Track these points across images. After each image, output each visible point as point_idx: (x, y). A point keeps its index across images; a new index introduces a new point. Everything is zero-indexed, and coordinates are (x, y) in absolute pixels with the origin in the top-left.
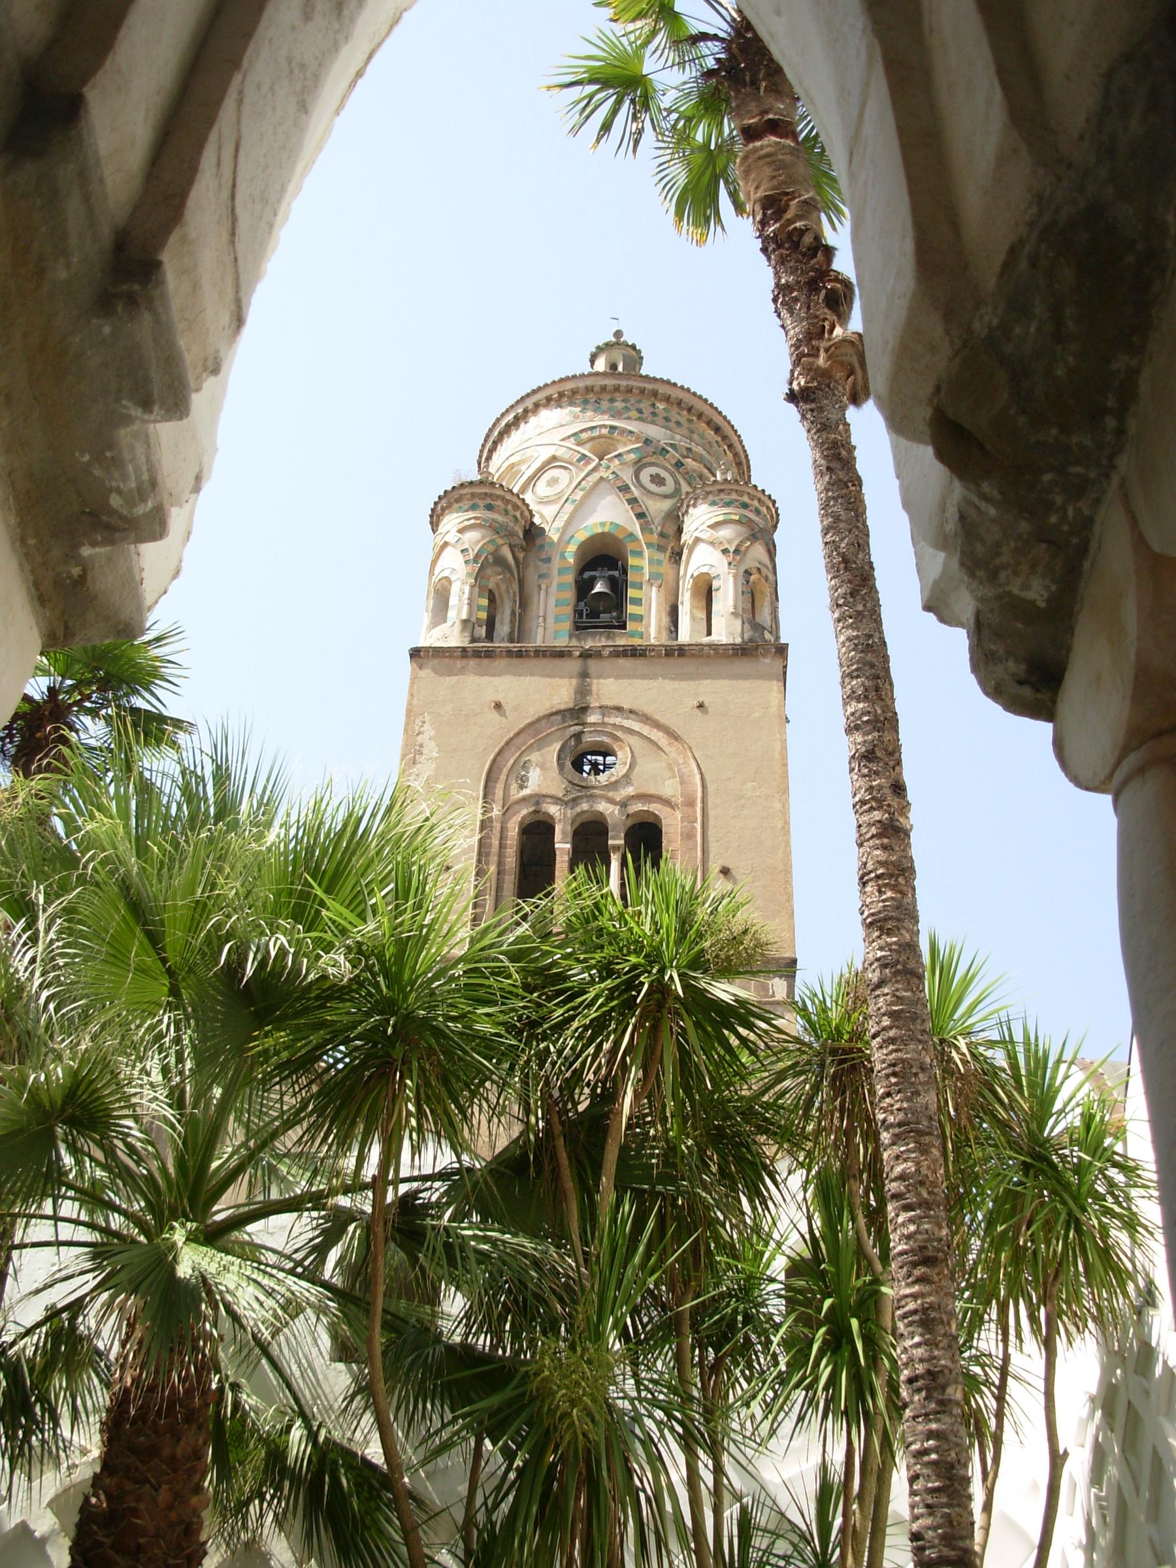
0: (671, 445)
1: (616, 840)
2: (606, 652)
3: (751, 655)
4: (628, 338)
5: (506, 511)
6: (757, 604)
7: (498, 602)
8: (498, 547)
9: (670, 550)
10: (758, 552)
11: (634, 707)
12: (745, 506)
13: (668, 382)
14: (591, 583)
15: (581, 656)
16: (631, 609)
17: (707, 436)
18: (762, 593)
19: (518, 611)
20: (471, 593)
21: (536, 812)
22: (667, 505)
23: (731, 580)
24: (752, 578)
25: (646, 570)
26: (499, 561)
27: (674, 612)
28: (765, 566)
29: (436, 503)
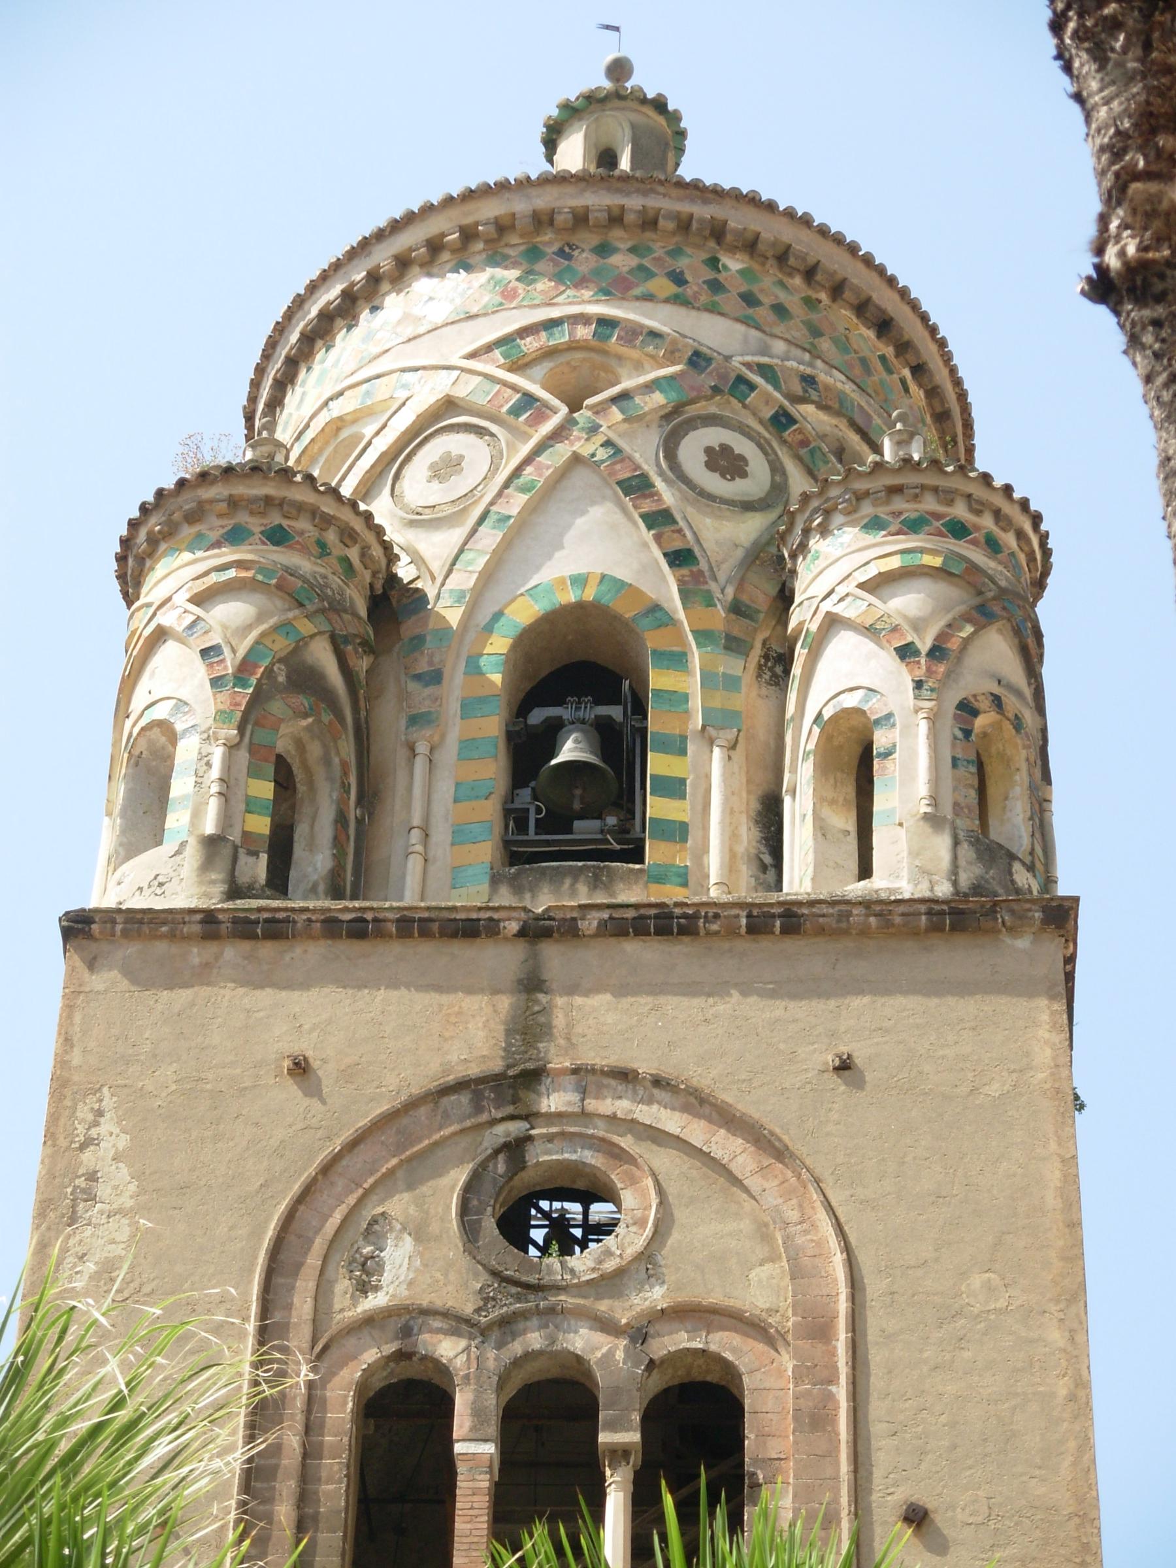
0: (765, 371)
1: (620, 1433)
2: (589, 925)
3: (979, 930)
4: (646, 80)
5: (322, 545)
6: (992, 791)
7: (301, 788)
8: (302, 644)
9: (757, 652)
10: (995, 651)
12: (958, 530)
13: (753, 200)
14: (550, 737)
15: (522, 933)
16: (656, 807)
17: (855, 343)
18: (1007, 761)
19: (353, 813)
21: (402, 1356)
22: (749, 529)
23: (923, 727)
24: (980, 722)
25: (696, 703)
26: (304, 679)
27: (770, 817)
28: (1019, 693)
29: (133, 525)
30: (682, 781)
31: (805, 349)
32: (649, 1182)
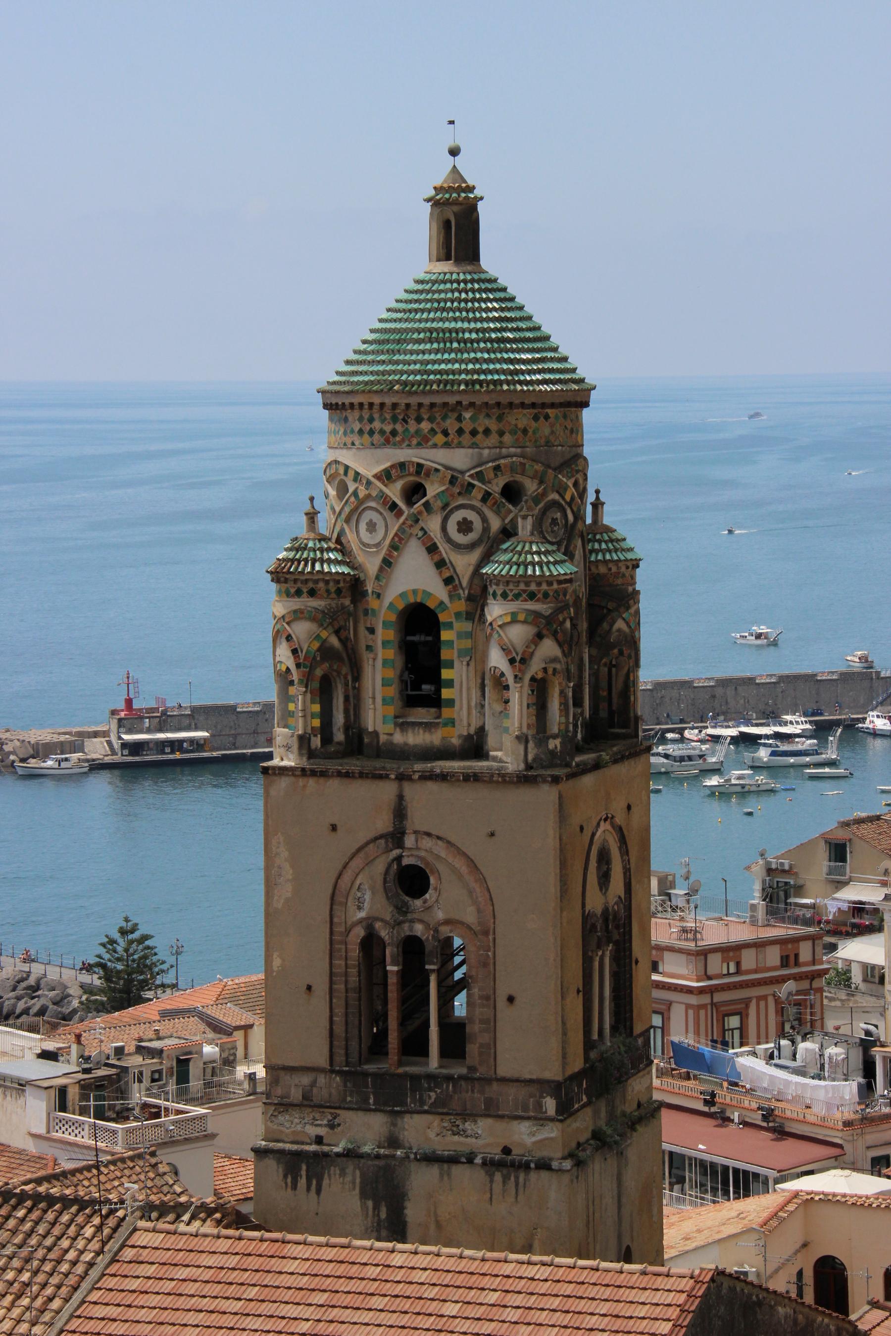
2: (416, 776)
5: (328, 591)
7: (333, 684)
11: (440, 834)
12: (532, 596)
20: (304, 702)
30: (452, 680)
31: (496, 447)
32: (437, 875)
